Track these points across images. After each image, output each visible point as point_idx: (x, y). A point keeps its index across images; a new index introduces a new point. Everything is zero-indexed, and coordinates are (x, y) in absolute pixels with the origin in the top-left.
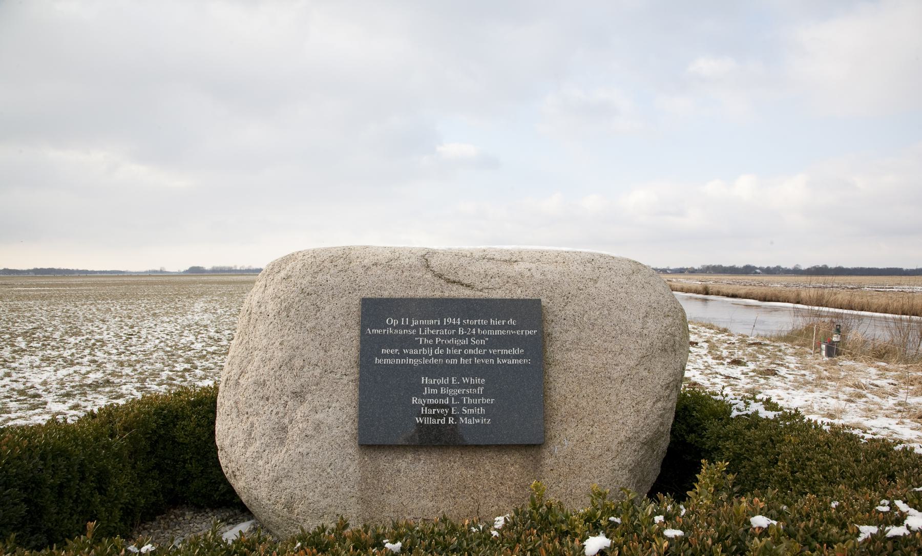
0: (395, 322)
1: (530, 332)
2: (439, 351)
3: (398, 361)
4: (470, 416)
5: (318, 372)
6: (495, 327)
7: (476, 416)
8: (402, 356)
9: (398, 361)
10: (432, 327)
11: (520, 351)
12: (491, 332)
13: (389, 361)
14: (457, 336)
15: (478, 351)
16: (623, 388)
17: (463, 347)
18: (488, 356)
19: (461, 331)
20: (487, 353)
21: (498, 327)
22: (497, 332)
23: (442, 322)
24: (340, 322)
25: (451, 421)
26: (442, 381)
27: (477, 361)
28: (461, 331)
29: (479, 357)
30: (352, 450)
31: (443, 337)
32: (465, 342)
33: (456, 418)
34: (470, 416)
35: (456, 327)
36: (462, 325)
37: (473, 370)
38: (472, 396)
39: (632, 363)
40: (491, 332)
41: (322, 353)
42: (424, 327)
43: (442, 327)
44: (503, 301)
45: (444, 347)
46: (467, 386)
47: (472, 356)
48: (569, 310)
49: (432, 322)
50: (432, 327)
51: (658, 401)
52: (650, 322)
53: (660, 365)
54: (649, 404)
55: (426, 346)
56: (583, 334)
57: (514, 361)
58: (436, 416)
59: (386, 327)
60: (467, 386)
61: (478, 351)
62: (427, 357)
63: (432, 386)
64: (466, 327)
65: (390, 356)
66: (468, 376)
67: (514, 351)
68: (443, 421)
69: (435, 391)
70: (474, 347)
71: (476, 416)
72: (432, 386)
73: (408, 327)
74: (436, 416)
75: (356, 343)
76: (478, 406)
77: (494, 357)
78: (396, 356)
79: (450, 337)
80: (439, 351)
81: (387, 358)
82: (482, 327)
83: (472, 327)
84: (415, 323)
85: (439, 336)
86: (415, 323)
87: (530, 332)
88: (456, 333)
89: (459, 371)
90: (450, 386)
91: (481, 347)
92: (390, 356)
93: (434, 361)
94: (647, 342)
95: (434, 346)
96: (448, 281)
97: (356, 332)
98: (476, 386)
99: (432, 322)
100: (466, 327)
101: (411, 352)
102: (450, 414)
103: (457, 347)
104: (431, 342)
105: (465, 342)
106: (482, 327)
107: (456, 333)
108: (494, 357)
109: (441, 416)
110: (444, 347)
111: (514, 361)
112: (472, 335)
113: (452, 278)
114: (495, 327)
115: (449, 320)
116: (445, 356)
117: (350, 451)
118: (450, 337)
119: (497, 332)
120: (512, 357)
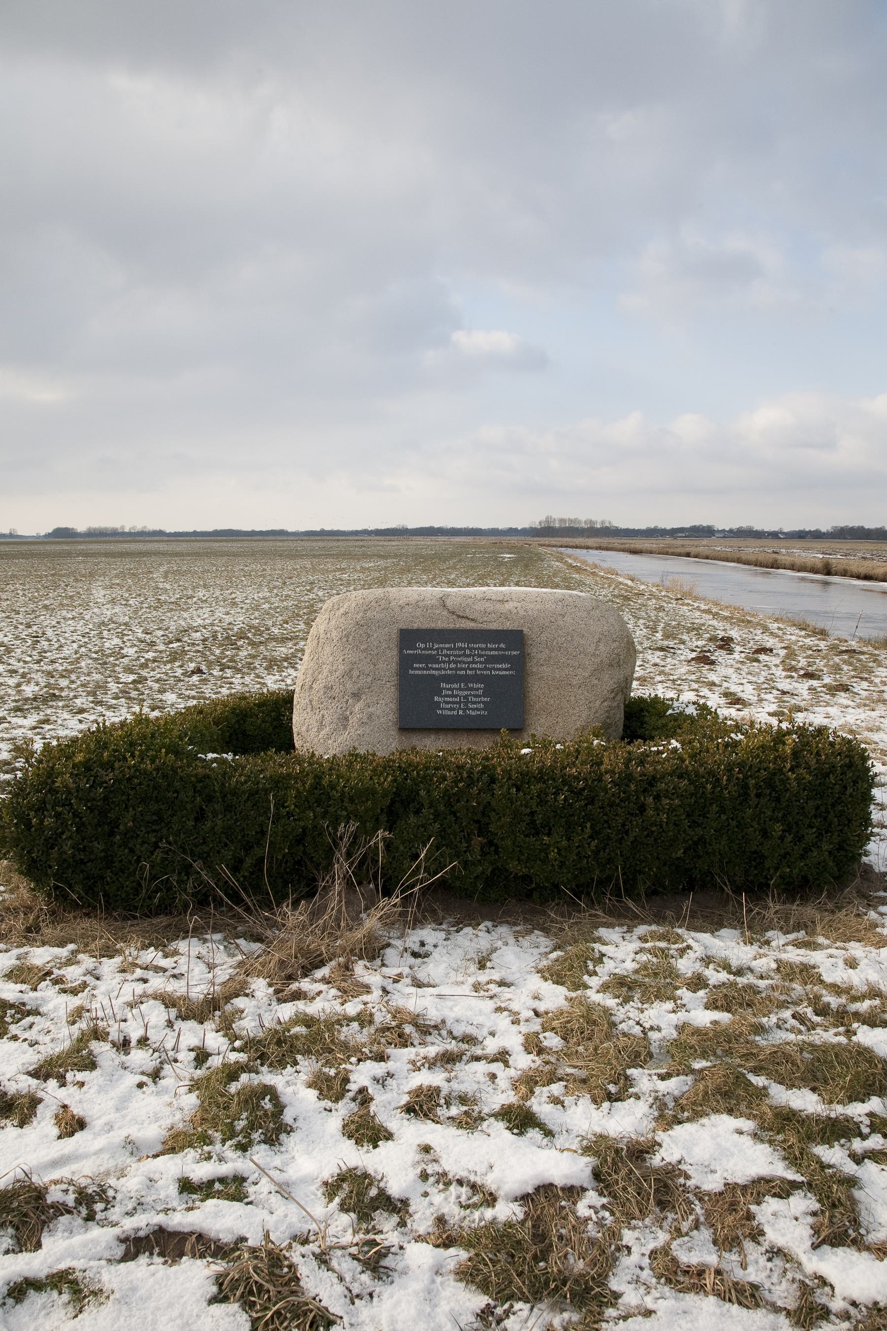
0: (422, 646)
1: (515, 653)
2: (453, 666)
3: (425, 672)
4: (473, 709)
5: (369, 679)
6: (491, 650)
7: (478, 709)
8: (428, 669)
9: (425, 672)
10: (448, 649)
11: (508, 666)
12: (488, 653)
13: (419, 672)
14: (465, 655)
15: (479, 666)
16: (580, 691)
17: (469, 663)
18: (486, 669)
19: (468, 652)
20: (485, 667)
21: (493, 649)
22: (493, 653)
23: (455, 645)
24: (384, 645)
25: (461, 712)
26: (455, 686)
27: (478, 672)
28: (468, 652)
29: (480, 669)
30: (394, 732)
31: (455, 656)
32: (471, 659)
33: (464, 710)
34: (473, 709)
35: (464, 649)
36: (468, 648)
37: (476, 679)
38: (475, 696)
39: (587, 675)
40: (488, 653)
41: (372, 666)
42: (442, 649)
43: (455, 649)
44: (497, 631)
45: (456, 662)
46: (472, 689)
47: (475, 669)
48: (544, 637)
49: (447, 646)
50: (448, 649)
51: (604, 701)
52: (602, 646)
53: (607, 676)
54: (598, 703)
55: (444, 662)
56: (553, 654)
57: (504, 673)
58: (451, 709)
59: (416, 649)
60: (472, 689)
61: (479, 666)
62: (445, 669)
63: (448, 689)
64: (471, 649)
65: (419, 669)
66: (473, 683)
67: (504, 666)
68: (455, 713)
69: (450, 693)
70: (476, 663)
71: (478, 709)
72: (448, 689)
73: (431, 649)
74: (451, 709)
75: (396, 659)
76: (479, 703)
77: (490, 670)
78: (423, 669)
79: (460, 656)
80: (453, 666)
81: (418, 670)
82: (482, 649)
83: (475, 649)
84: (436, 646)
85: (452, 655)
86: (436, 646)
87: (515, 653)
88: (464, 653)
89: (466, 679)
90: (460, 689)
91: (481, 663)
92: (419, 669)
93: (449, 672)
94: (598, 660)
95: (449, 662)
96: (459, 616)
97: (395, 652)
98: (477, 689)
99: (447, 646)
100: (471, 649)
101: (434, 666)
102: (460, 708)
103: (465, 663)
104: (447, 659)
105: (471, 659)
106: (482, 649)
107: (464, 653)
108: (490, 670)
109: (454, 709)
110: (456, 662)
111: (504, 673)
112: (475, 655)
113: (461, 614)
114: (491, 650)
115: (460, 644)
116: (456, 669)
117: (393, 733)
118: (460, 656)
119: (493, 653)
120: (502, 670)
